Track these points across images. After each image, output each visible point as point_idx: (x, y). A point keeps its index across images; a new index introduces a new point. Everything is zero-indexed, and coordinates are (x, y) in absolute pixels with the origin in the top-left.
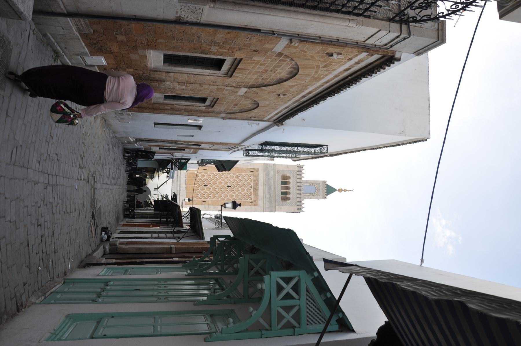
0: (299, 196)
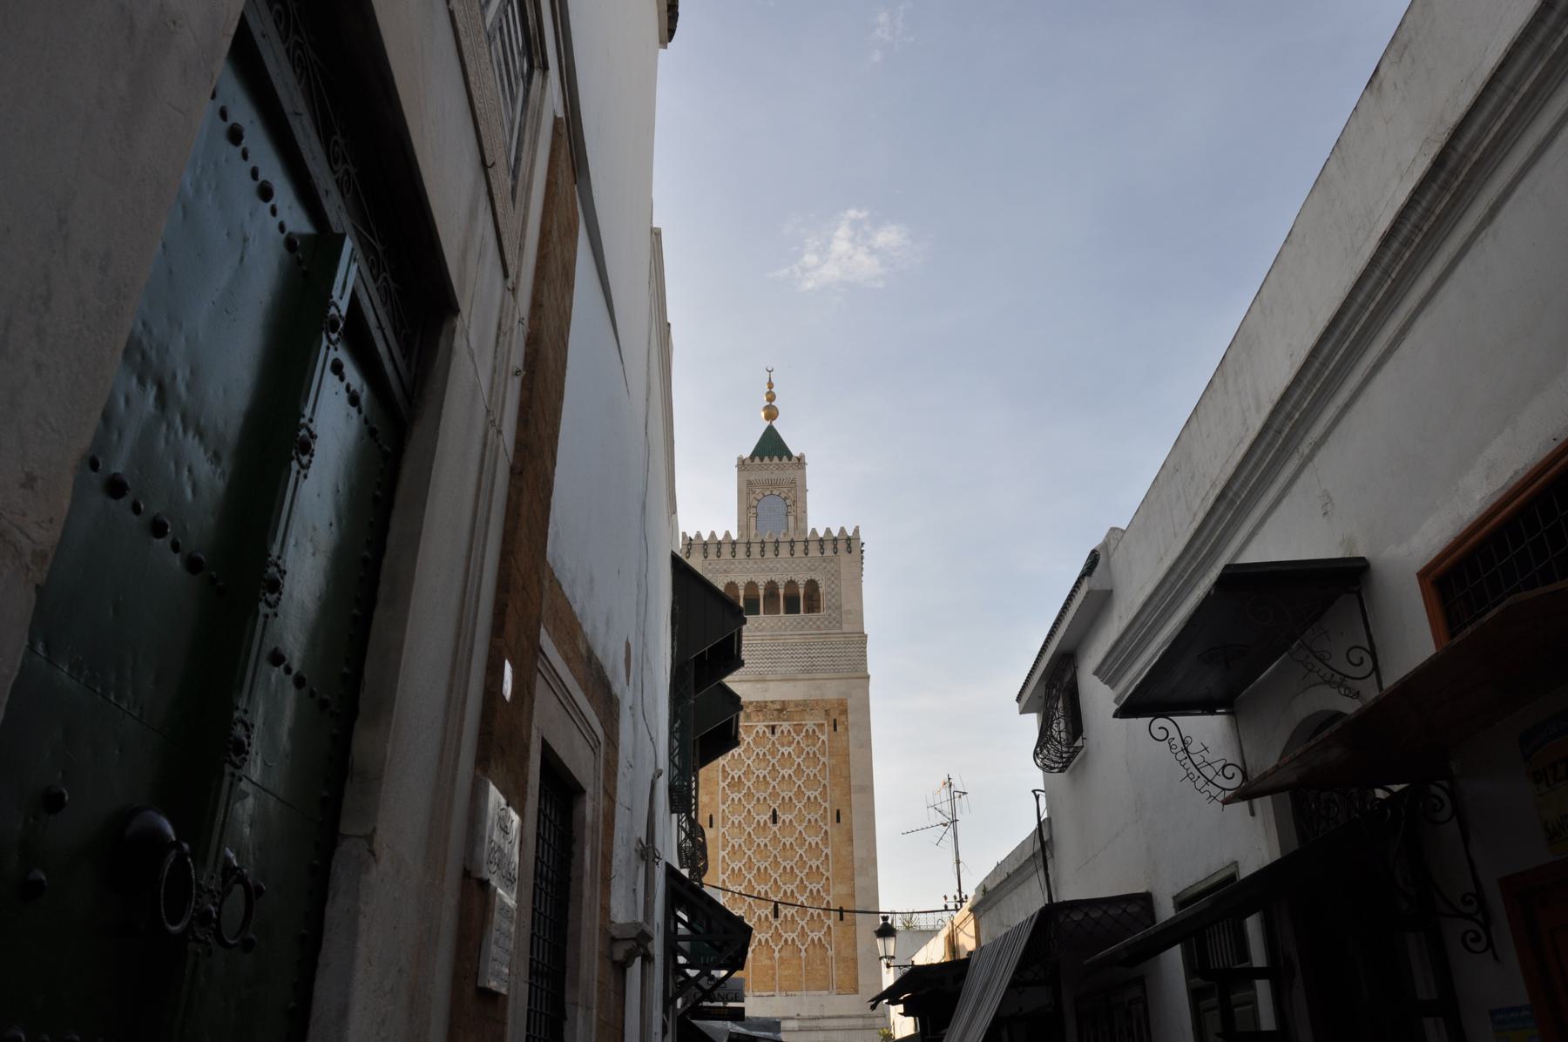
0: (799, 547)
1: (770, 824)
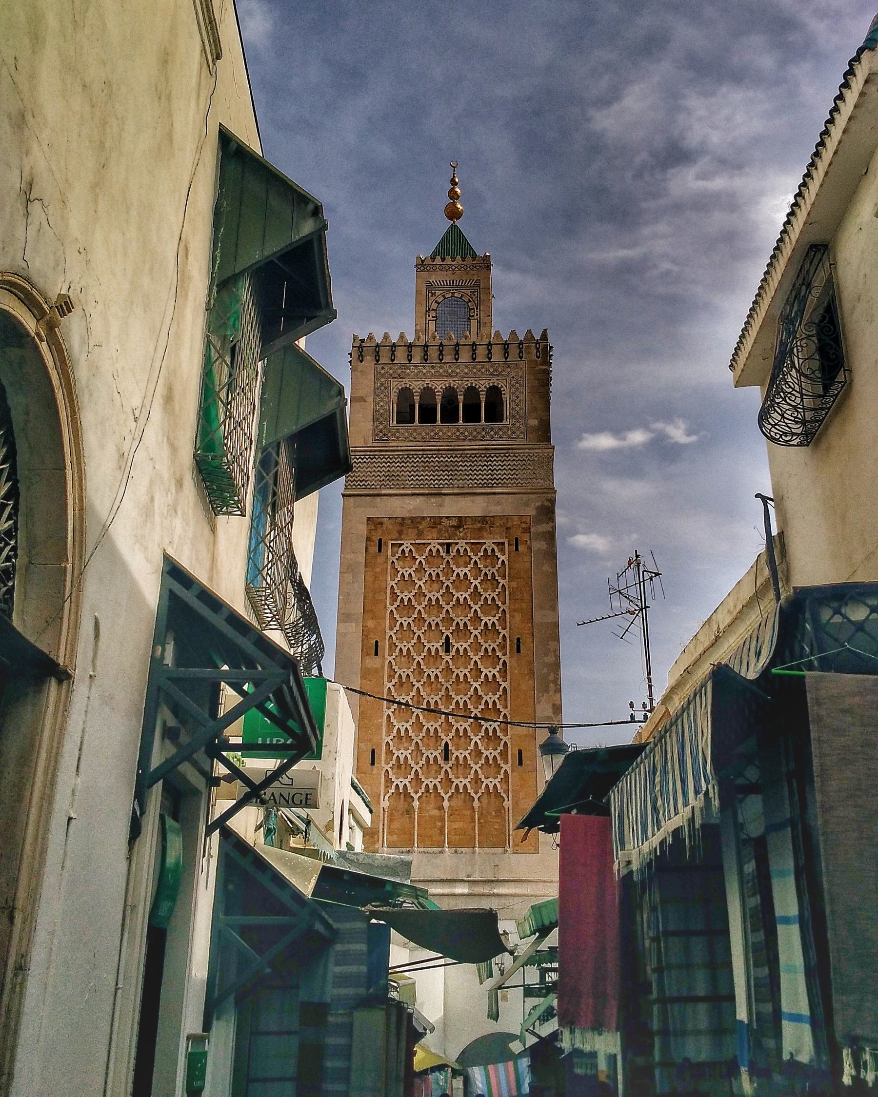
0: (481, 351)
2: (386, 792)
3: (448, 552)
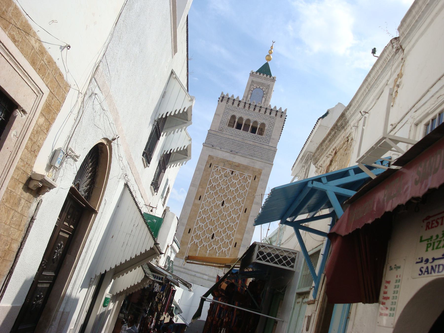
0: (263, 110)
1: (220, 206)
2: (190, 243)
3: (232, 174)
